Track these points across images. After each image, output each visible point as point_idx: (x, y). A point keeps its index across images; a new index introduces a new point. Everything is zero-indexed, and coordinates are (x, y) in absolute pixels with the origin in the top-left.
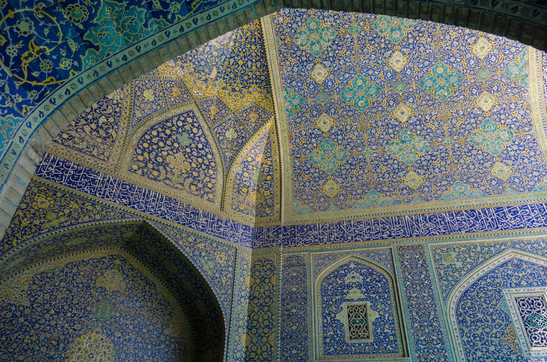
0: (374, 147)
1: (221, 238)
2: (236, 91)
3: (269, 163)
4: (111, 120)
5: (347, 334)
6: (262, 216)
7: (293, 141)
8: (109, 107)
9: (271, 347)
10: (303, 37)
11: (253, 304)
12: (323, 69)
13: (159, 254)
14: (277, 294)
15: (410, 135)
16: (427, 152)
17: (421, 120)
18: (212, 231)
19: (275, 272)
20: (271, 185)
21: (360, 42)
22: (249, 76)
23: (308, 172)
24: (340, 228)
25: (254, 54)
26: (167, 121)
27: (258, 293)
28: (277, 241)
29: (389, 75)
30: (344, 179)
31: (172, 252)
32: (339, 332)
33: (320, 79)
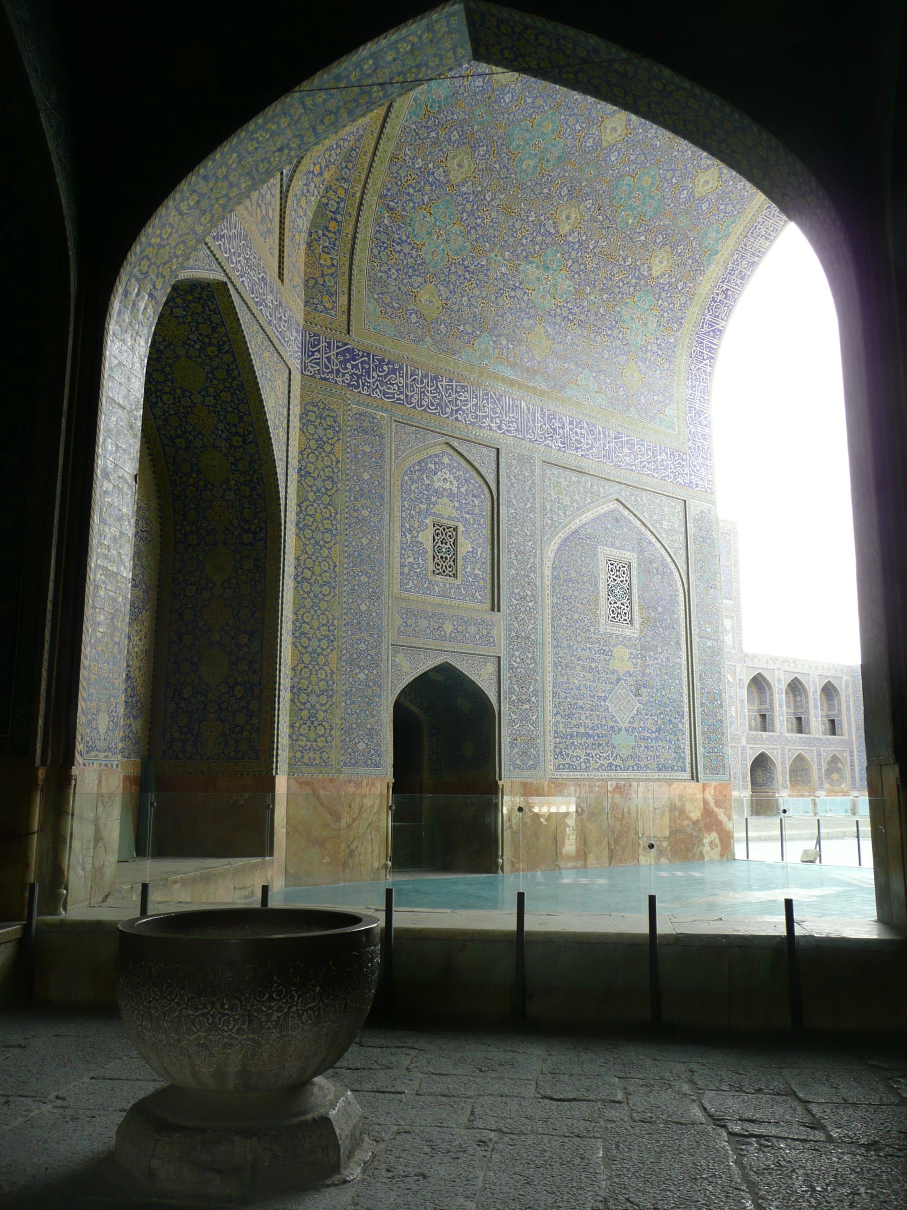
5: (431, 567)
6: (316, 309)
7: (394, 169)
9: (335, 566)
11: (305, 486)
13: (185, 343)
14: (343, 477)
15: (559, 261)
16: (567, 303)
19: (340, 435)
20: (334, 245)
23: (398, 248)
24: (437, 387)
27: (313, 467)
28: (344, 375)
30: (451, 292)
31: (228, 358)
32: (420, 561)
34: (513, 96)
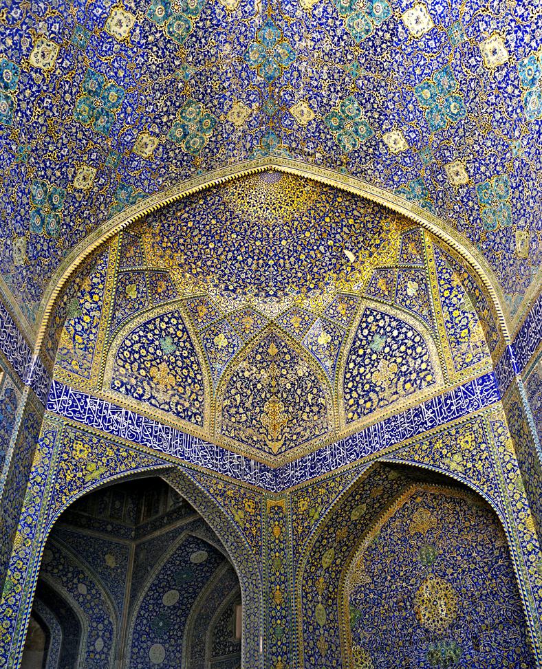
0: (517, 134)
1: (457, 417)
2: (379, 245)
3: (466, 275)
4: (315, 391)
8: (307, 382)
10: (345, 139)
12: (391, 134)
17: (519, 27)
18: (443, 419)
21: (373, 69)
22: (369, 221)
25: (347, 203)
26: (354, 343)
29: (432, 44)
33: (402, 145)
34: (411, 131)
